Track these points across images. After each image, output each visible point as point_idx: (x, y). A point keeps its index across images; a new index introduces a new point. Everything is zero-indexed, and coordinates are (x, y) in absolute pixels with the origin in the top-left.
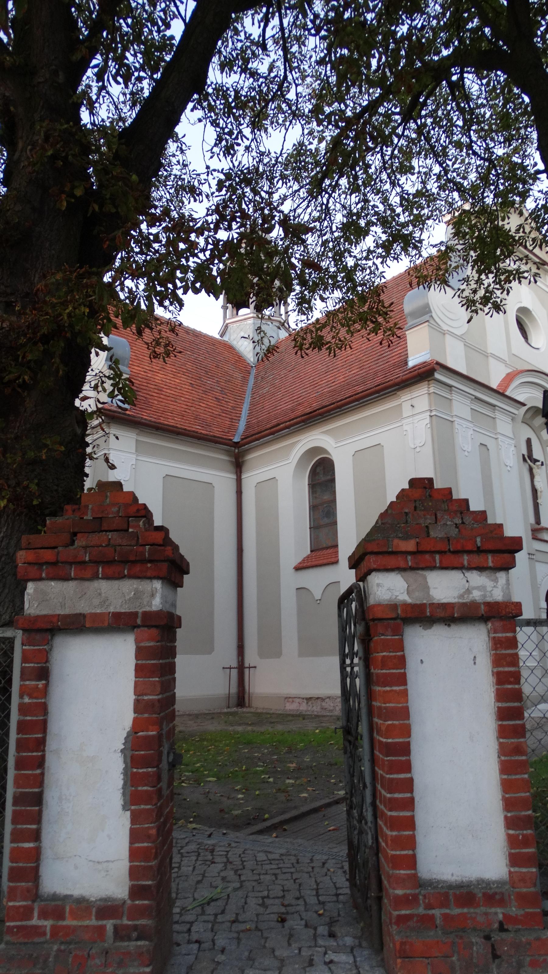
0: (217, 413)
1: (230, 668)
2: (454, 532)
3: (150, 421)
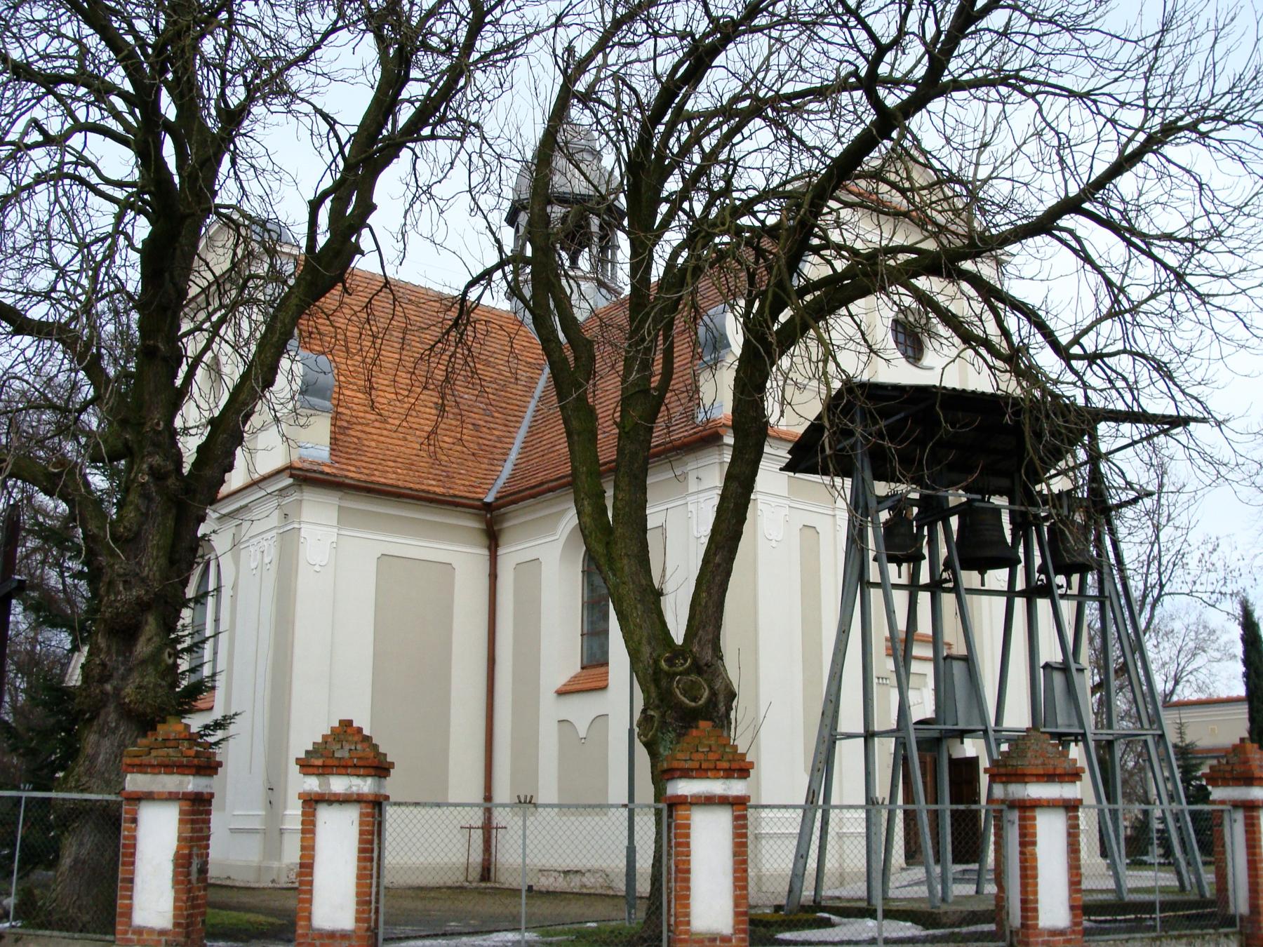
1: (470, 828)
2: (347, 755)
3: (359, 480)
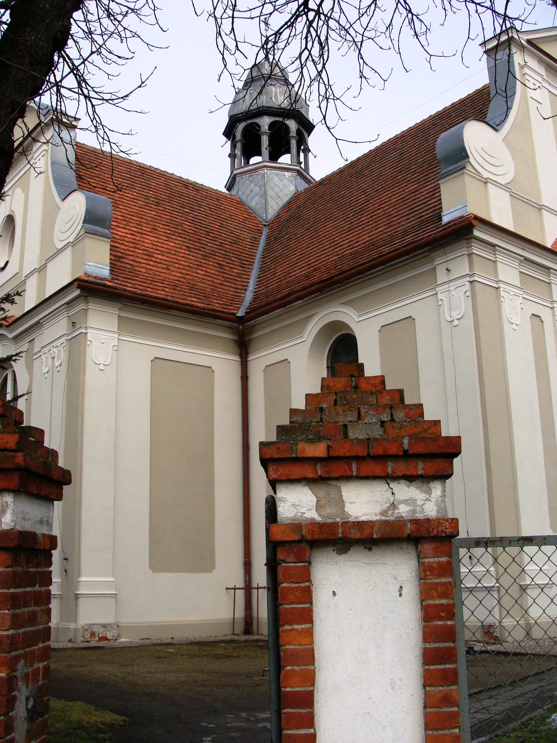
0: (219, 282)
1: (235, 589)
2: (378, 432)
